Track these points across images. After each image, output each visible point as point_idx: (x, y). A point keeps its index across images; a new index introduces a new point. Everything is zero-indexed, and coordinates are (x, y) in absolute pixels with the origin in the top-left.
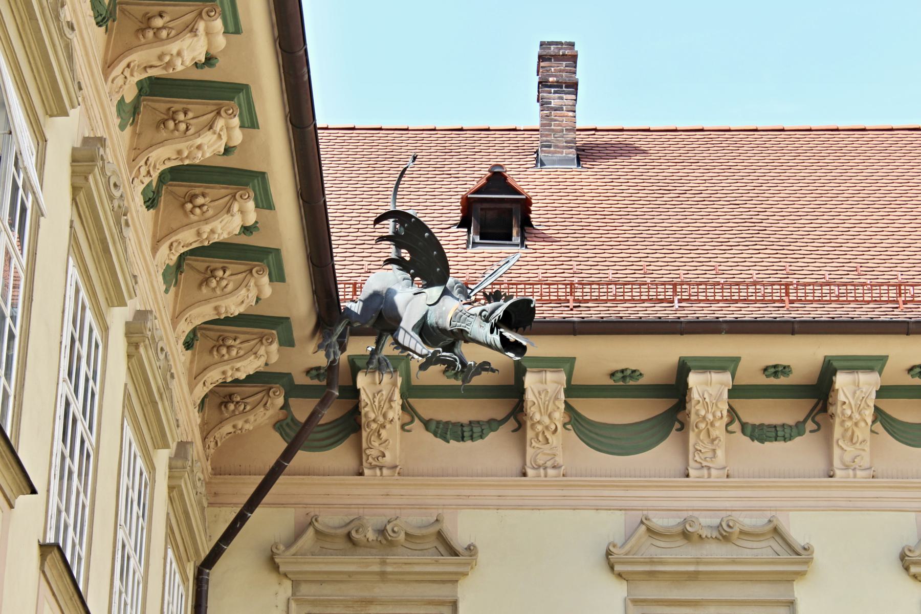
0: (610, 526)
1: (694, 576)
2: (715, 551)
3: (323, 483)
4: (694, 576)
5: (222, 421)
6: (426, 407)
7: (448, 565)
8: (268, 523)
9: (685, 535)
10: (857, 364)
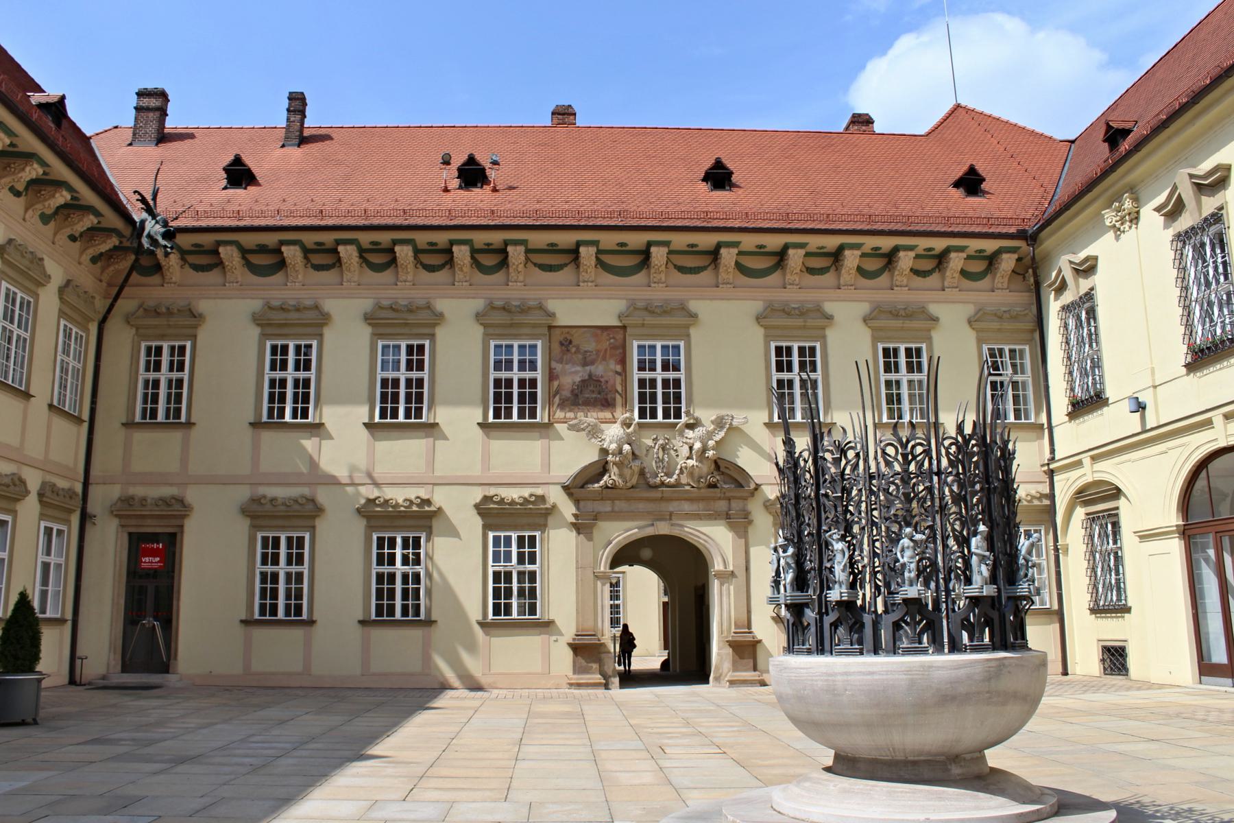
0: (256, 305)
1: (285, 325)
2: (294, 316)
3: (147, 291)
4: (285, 325)
5: (109, 266)
6: (192, 259)
7: (192, 321)
9: (282, 309)
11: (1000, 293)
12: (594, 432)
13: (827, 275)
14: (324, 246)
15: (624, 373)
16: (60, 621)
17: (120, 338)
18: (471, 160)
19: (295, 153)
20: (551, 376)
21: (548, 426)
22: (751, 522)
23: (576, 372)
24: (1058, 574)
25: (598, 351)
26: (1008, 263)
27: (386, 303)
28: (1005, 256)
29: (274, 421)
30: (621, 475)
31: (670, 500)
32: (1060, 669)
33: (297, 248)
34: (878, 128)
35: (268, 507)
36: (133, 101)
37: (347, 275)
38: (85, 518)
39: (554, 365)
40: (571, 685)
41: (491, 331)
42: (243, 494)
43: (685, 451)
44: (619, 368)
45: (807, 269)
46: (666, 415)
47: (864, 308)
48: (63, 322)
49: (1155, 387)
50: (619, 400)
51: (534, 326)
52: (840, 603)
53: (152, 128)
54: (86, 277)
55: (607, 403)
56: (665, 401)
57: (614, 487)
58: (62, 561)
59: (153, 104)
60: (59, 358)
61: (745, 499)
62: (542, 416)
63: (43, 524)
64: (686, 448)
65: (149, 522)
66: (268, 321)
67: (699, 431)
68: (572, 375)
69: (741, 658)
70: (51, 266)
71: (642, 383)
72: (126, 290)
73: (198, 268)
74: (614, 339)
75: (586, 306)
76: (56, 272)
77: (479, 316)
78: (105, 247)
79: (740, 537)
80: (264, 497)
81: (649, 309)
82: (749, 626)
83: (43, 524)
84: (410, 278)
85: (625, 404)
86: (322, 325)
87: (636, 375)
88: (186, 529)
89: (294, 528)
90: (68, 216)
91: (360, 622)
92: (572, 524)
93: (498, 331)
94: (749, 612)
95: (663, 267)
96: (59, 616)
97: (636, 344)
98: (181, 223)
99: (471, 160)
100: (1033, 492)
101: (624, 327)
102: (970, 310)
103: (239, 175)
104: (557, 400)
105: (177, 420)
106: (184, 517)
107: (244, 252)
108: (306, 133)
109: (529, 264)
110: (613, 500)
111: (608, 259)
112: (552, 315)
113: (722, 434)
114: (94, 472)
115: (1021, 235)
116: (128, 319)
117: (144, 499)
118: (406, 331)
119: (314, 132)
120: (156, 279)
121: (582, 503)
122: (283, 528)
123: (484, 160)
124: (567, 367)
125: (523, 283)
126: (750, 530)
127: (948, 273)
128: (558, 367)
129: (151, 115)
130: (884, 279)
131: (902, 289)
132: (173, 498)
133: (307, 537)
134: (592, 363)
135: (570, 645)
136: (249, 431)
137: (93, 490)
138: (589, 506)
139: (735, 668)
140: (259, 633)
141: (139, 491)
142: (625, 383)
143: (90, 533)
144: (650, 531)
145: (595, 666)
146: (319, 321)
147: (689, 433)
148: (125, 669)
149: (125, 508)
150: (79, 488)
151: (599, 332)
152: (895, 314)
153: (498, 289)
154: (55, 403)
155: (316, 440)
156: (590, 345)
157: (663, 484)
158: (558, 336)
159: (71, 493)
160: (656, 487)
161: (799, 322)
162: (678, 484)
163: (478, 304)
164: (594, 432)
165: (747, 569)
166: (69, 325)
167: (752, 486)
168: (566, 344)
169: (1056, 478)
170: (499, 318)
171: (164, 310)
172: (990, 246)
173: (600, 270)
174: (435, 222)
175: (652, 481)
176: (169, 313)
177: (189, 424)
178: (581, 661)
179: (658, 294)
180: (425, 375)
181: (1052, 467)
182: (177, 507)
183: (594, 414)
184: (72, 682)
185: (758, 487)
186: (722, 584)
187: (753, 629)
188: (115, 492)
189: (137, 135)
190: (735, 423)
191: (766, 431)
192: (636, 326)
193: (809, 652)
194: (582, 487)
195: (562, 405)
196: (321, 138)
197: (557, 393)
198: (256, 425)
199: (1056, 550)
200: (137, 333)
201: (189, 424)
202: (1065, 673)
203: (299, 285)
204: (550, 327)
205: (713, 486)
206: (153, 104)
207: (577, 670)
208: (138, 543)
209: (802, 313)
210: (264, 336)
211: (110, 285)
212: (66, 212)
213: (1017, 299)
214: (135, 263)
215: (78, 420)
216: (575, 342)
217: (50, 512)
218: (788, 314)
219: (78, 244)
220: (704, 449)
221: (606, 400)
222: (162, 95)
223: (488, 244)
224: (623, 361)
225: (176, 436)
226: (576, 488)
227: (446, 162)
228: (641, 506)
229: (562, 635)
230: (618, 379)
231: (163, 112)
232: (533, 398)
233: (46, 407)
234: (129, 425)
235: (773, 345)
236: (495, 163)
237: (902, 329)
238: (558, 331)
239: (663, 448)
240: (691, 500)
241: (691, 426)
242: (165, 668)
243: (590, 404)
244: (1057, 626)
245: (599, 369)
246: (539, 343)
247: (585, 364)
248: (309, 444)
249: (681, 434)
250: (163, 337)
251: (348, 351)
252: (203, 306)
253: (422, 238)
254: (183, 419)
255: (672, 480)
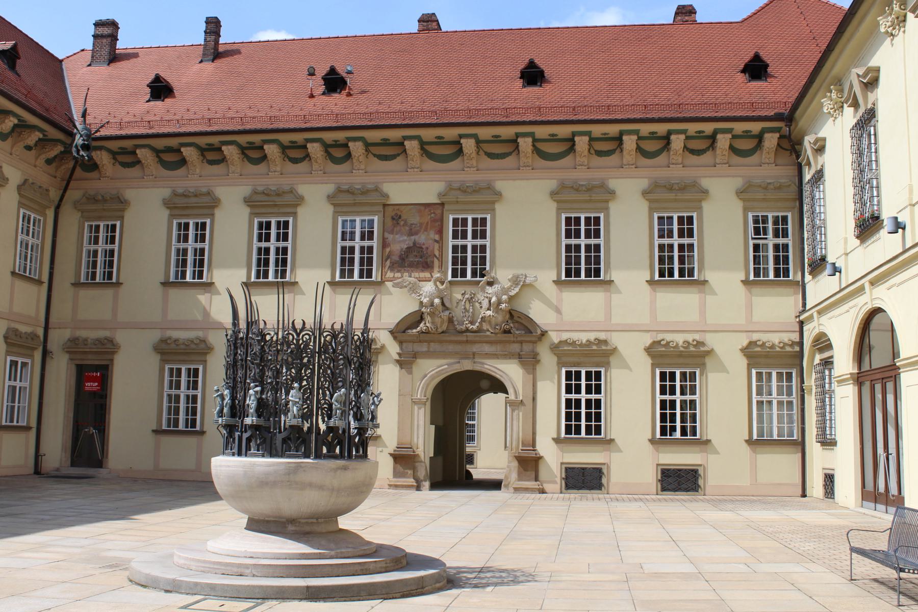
0: (166, 193)
1: (187, 207)
2: (194, 200)
4: (187, 207)
6: (121, 158)
8: (73, 194)
10: (630, 132)
11: (767, 168)
12: (414, 289)
13: (613, 156)
14: (212, 146)
15: (441, 241)
16: (27, 428)
17: (70, 220)
18: (333, 71)
19: (209, 66)
20: (384, 244)
21: (381, 283)
22: (538, 361)
23: (404, 241)
24: (803, 410)
25: (421, 224)
26: (771, 140)
27: (260, 189)
28: (767, 136)
29: (179, 283)
30: (433, 323)
31: (474, 342)
32: (800, 492)
33: (192, 148)
34: (700, 18)
35: (173, 346)
36: (91, 30)
37: (232, 168)
38: (45, 353)
39: (386, 235)
40: (390, 485)
41: (339, 209)
42: (155, 336)
43: (485, 304)
44: (437, 237)
45: (596, 151)
46: (474, 274)
47: (644, 183)
48: (22, 211)
49: (847, 254)
50: (436, 263)
51: (373, 204)
52: (252, 426)
53: (105, 51)
54: (42, 176)
55: (427, 266)
56: (473, 265)
57: (427, 332)
58: (27, 385)
59: (107, 31)
60: (19, 238)
61: (534, 342)
62: (376, 276)
63: (9, 359)
64: (487, 301)
65: (90, 357)
66: (177, 205)
67: (496, 288)
68: (400, 243)
69: (526, 470)
70: (8, 171)
71: (455, 248)
72: (72, 184)
73: (125, 165)
74: (433, 213)
75: (414, 188)
76: (14, 176)
77: (330, 198)
78: (52, 154)
79: (529, 373)
80: (170, 338)
81: (463, 190)
82: (534, 444)
83: (9, 359)
84: (278, 169)
85: (441, 266)
86: (213, 207)
87: (451, 242)
88: (115, 362)
89: (192, 362)
90: (20, 134)
91: (153, 431)
92: (397, 361)
93: (345, 209)
94: (534, 433)
95: (474, 155)
96: (25, 424)
97: (451, 217)
98: (103, 132)
99: (333, 71)
100: (786, 340)
101: (442, 204)
102: (738, 182)
103: (160, 89)
104: (388, 263)
105: (110, 281)
106: (113, 353)
107: (157, 152)
108: (221, 49)
109: (370, 155)
110: (429, 342)
111: (432, 149)
112: (387, 196)
113: (517, 290)
114: (53, 319)
115: (778, 117)
116: (76, 205)
117: (86, 340)
118: (275, 210)
119: (228, 48)
120: (94, 174)
121: (404, 345)
122: (184, 362)
123: (341, 70)
124: (397, 236)
125: (363, 172)
126: (538, 368)
127: (718, 152)
128: (390, 237)
129: (104, 41)
130: (662, 159)
131: (675, 167)
132: (106, 338)
133: (201, 368)
134: (416, 233)
135: (391, 455)
136: (160, 289)
137: (52, 334)
138: (409, 347)
139: (520, 478)
140: (166, 440)
141: (83, 334)
142: (441, 249)
143: (51, 366)
144: (457, 368)
145: (410, 472)
146: (211, 204)
147: (490, 290)
148: (73, 464)
149: (74, 346)
150: (40, 332)
151: (422, 208)
152: (670, 188)
153: (345, 176)
154: (17, 271)
155: (208, 295)
156: (415, 219)
157: (467, 330)
158: (390, 212)
159: (34, 336)
160: (462, 332)
161: (586, 197)
162: (479, 330)
163: (330, 188)
164: (414, 289)
165: (534, 399)
166: (28, 213)
167: (539, 332)
168: (397, 219)
169: (805, 328)
170: (348, 199)
171: (100, 198)
172: (755, 127)
173: (425, 158)
174: (292, 126)
175: (459, 327)
176: (104, 200)
177: (118, 284)
178: (399, 468)
179: (470, 177)
180: (289, 244)
181: (802, 318)
182: (109, 346)
183: (417, 275)
184: (37, 471)
185: (544, 333)
186: (513, 411)
187: (538, 447)
188: (67, 334)
189: (94, 60)
190: (528, 281)
191: (554, 287)
192: (450, 203)
193: (233, 455)
194: (404, 332)
195: (392, 268)
196: (232, 52)
197: (388, 257)
198: (166, 284)
199: (803, 390)
200: (82, 216)
201: (118, 284)
202: (804, 495)
203: (197, 176)
204: (385, 205)
205: (507, 332)
206: (107, 31)
207: (396, 474)
208: (82, 372)
209: (590, 189)
210: (172, 216)
211: (63, 180)
212: (19, 130)
213: (781, 173)
214: (78, 166)
215: (39, 282)
216: (404, 217)
217: (15, 349)
218: (577, 190)
219: (33, 152)
220: (499, 302)
221: (426, 263)
222: (114, 25)
223: (336, 141)
224: (440, 232)
225: (109, 292)
226: (400, 332)
227: (312, 74)
228: (451, 347)
229: (386, 447)
230: (437, 246)
231: (114, 38)
232: (370, 261)
233: (9, 274)
234: (77, 284)
235: (563, 216)
236: (349, 72)
237: (676, 200)
238: (390, 209)
239: (470, 300)
240: (491, 343)
241: (490, 284)
242: (99, 463)
243: (414, 266)
244: (800, 455)
245: (421, 238)
246: (376, 219)
247: (411, 233)
248: (203, 298)
249: (483, 290)
250: (100, 218)
251: (232, 228)
252: (129, 194)
253: (285, 138)
254: (114, 280)
255: (475, 327)
